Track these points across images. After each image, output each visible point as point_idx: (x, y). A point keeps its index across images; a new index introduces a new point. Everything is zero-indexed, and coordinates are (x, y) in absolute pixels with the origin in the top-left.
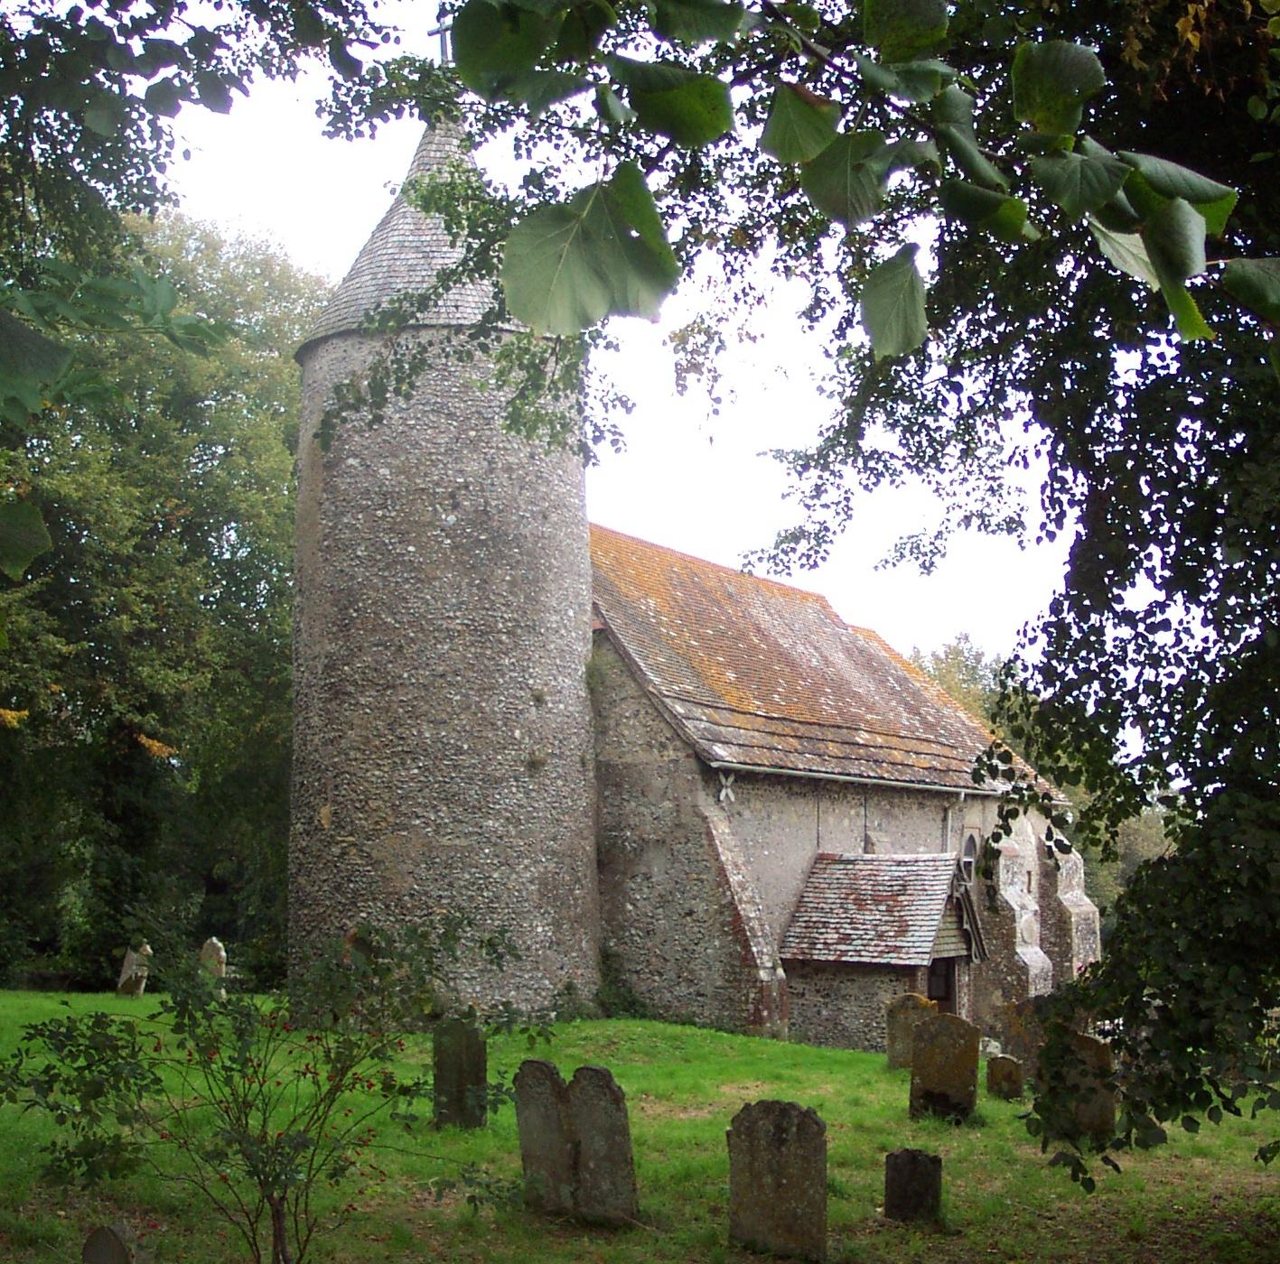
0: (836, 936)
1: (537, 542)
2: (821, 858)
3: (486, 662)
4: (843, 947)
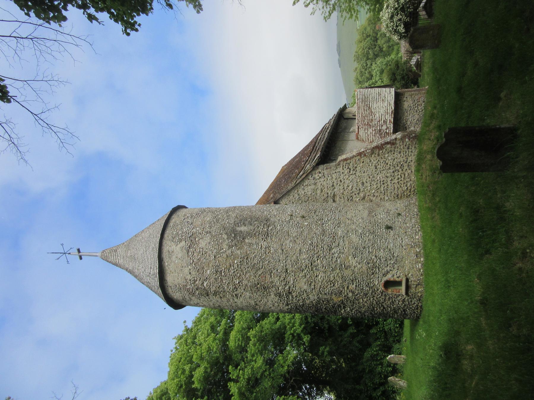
0: (384, 125)
1: (238, 218)
2: (357, 138)
3: (278, 234)
4: (388, 122)
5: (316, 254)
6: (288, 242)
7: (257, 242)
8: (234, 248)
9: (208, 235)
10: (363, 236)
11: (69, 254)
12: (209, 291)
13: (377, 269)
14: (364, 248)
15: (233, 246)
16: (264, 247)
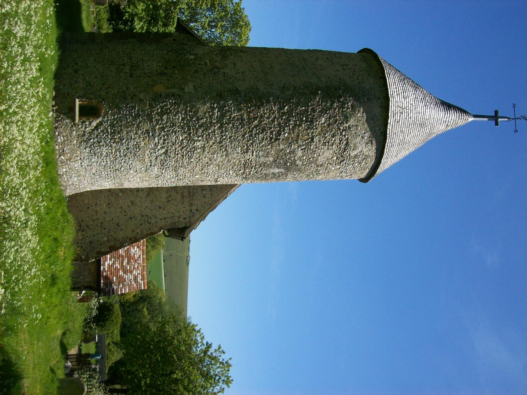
5: (184, 147)
6: (219, 159)
7: (258, 158)
8: (288, 151)
9: (321, 163)
10: (128, 167)
11: (510, 118)
12: (325, 94)
13: (109, 131)
14: (125, 156)
15: (289, 153)
16: (249, 153)
